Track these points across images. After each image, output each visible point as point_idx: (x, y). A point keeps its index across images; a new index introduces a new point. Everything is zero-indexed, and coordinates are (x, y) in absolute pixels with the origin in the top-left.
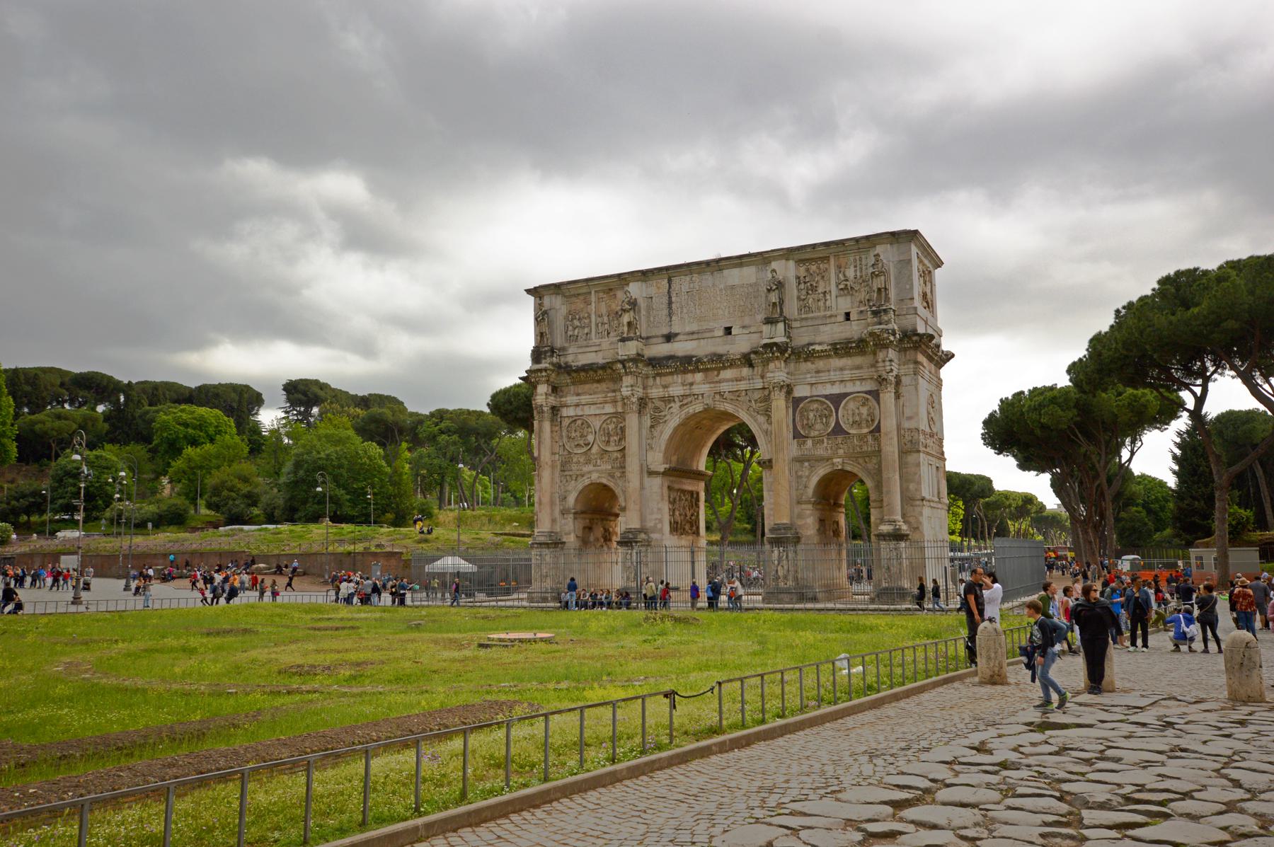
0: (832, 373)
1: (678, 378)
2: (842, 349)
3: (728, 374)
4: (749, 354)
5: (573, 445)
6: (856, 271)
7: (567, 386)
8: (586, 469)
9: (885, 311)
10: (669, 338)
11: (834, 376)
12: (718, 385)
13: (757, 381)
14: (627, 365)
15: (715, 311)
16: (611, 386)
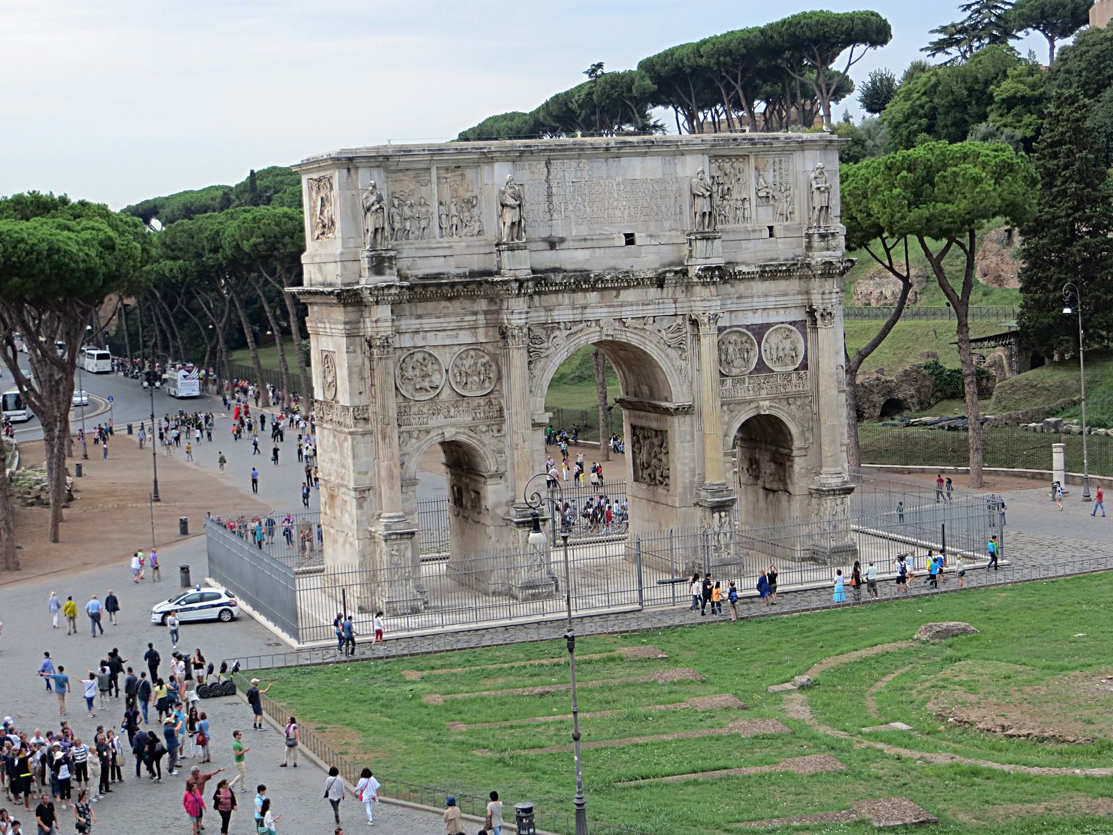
0: (755, 299)
1: (565, 298)
2: (769, 273)
3: (629, 295)
4: (665, 272)
5: (410, 388)
6: (775, 176)
7: (401, 303)
8: (433, 422)
9: (833, 234)
10: (552, 244)
11: (757, 303)
12: (619, 309)
13: (667, 306)
14: (525, 285)
15: (611, 211)
16: (468, 305)
